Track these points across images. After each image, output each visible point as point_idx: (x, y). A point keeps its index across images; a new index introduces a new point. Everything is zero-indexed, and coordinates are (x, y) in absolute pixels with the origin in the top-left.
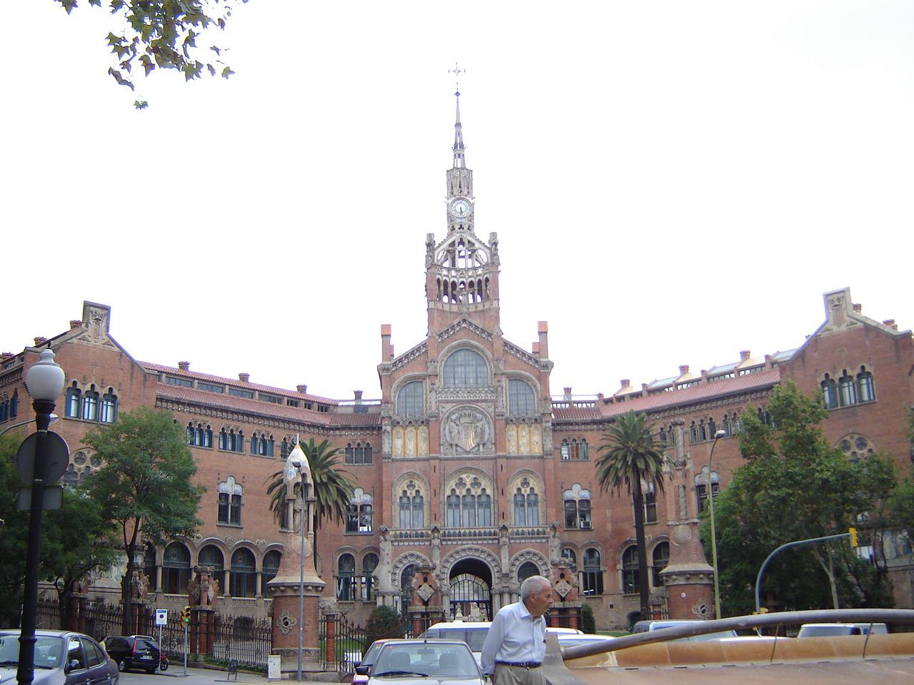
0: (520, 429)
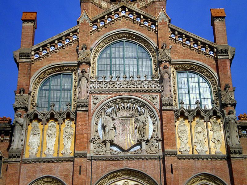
0: (194, 124)
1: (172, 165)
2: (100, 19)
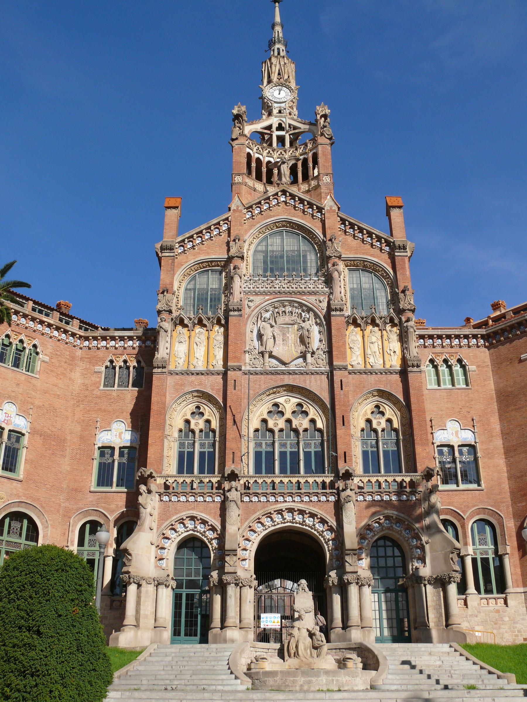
1: (341, 381)
2: (256, 204)
